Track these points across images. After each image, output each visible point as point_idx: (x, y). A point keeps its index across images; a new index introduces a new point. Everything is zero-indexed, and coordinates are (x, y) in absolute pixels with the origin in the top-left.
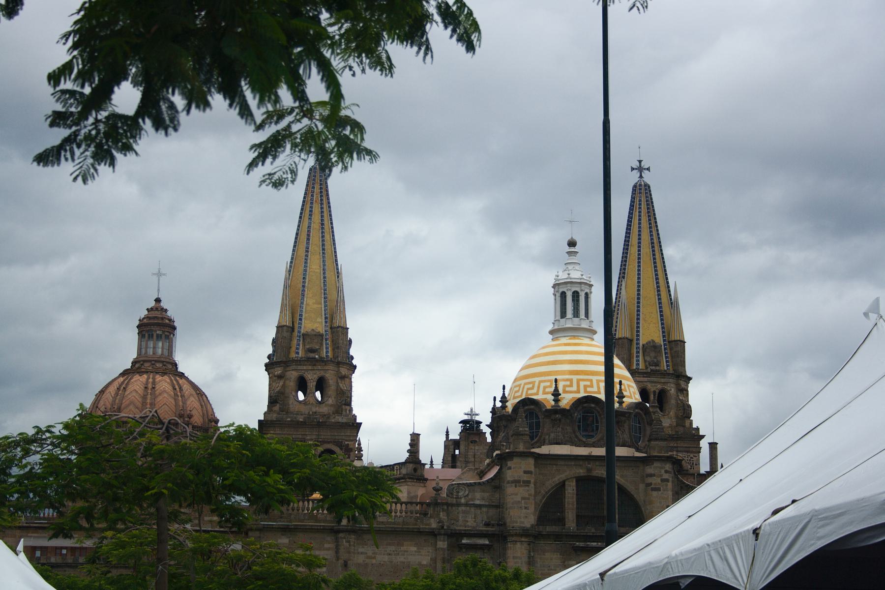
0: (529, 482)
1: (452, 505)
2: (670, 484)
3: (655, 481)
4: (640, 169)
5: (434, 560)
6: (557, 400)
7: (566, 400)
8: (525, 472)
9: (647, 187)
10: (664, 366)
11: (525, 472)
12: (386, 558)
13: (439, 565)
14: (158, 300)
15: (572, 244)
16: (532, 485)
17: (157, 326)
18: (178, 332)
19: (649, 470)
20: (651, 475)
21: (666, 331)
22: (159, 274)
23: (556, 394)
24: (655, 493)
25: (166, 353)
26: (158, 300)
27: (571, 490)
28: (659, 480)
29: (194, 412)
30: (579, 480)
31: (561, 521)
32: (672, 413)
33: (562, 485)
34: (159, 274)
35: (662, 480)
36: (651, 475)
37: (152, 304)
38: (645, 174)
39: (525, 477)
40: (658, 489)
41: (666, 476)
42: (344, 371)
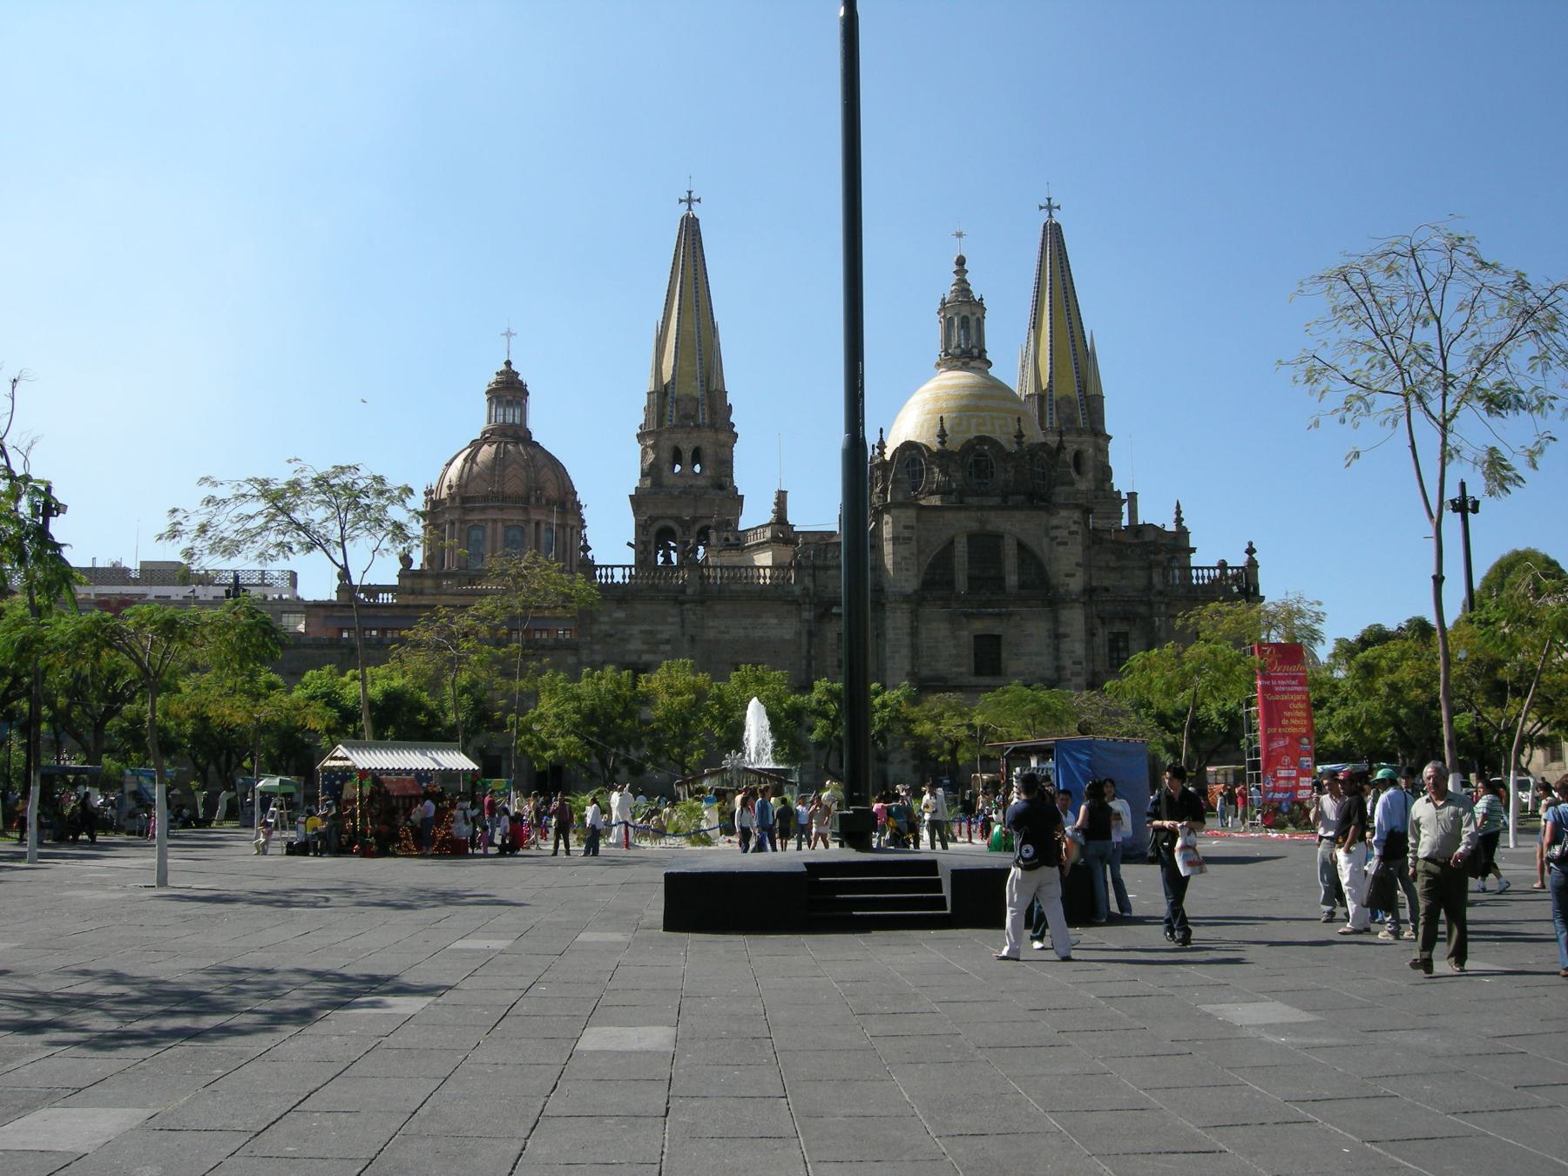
0: (910, 539)
1: (819, 568)
2: (1079, 537)
3: (1061, 534)
4: (1050, 208)
5: (799, 634)
6: (942, 443)
7: (954, 444)
8: (906, 527)
9: (1058, 226)
10: (1081, 423)
11: (906, 527)
12: (742, 633)
13: (804, 639)
14: (508, 363)
15: (961, 261)
16: (914, 543)
17: (509, 390)
18: (530, 398)
19: (1055, 521)
20: (1057, 527)
21: (1083, 385)
22: (509, 334)
23: (942, 435)
24: (1061, 549)
25: (517, 421)
26: (508, 363)
27: (961, 547)
28: (1065, 533)
29: (548, 485)
30: (971, 537)
31: (950, 584)
32: (1090, 476)
33: (952, 543)
34: (509, 334)
35: (1071, 533)
36: (1057, 527)
37: (504, 367)
38: (1055, 213)
39: (907, 533)
40: (1066, 544)
41: (1074, 528)
42: (722, 437)
